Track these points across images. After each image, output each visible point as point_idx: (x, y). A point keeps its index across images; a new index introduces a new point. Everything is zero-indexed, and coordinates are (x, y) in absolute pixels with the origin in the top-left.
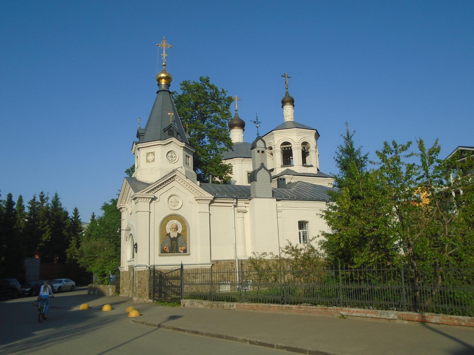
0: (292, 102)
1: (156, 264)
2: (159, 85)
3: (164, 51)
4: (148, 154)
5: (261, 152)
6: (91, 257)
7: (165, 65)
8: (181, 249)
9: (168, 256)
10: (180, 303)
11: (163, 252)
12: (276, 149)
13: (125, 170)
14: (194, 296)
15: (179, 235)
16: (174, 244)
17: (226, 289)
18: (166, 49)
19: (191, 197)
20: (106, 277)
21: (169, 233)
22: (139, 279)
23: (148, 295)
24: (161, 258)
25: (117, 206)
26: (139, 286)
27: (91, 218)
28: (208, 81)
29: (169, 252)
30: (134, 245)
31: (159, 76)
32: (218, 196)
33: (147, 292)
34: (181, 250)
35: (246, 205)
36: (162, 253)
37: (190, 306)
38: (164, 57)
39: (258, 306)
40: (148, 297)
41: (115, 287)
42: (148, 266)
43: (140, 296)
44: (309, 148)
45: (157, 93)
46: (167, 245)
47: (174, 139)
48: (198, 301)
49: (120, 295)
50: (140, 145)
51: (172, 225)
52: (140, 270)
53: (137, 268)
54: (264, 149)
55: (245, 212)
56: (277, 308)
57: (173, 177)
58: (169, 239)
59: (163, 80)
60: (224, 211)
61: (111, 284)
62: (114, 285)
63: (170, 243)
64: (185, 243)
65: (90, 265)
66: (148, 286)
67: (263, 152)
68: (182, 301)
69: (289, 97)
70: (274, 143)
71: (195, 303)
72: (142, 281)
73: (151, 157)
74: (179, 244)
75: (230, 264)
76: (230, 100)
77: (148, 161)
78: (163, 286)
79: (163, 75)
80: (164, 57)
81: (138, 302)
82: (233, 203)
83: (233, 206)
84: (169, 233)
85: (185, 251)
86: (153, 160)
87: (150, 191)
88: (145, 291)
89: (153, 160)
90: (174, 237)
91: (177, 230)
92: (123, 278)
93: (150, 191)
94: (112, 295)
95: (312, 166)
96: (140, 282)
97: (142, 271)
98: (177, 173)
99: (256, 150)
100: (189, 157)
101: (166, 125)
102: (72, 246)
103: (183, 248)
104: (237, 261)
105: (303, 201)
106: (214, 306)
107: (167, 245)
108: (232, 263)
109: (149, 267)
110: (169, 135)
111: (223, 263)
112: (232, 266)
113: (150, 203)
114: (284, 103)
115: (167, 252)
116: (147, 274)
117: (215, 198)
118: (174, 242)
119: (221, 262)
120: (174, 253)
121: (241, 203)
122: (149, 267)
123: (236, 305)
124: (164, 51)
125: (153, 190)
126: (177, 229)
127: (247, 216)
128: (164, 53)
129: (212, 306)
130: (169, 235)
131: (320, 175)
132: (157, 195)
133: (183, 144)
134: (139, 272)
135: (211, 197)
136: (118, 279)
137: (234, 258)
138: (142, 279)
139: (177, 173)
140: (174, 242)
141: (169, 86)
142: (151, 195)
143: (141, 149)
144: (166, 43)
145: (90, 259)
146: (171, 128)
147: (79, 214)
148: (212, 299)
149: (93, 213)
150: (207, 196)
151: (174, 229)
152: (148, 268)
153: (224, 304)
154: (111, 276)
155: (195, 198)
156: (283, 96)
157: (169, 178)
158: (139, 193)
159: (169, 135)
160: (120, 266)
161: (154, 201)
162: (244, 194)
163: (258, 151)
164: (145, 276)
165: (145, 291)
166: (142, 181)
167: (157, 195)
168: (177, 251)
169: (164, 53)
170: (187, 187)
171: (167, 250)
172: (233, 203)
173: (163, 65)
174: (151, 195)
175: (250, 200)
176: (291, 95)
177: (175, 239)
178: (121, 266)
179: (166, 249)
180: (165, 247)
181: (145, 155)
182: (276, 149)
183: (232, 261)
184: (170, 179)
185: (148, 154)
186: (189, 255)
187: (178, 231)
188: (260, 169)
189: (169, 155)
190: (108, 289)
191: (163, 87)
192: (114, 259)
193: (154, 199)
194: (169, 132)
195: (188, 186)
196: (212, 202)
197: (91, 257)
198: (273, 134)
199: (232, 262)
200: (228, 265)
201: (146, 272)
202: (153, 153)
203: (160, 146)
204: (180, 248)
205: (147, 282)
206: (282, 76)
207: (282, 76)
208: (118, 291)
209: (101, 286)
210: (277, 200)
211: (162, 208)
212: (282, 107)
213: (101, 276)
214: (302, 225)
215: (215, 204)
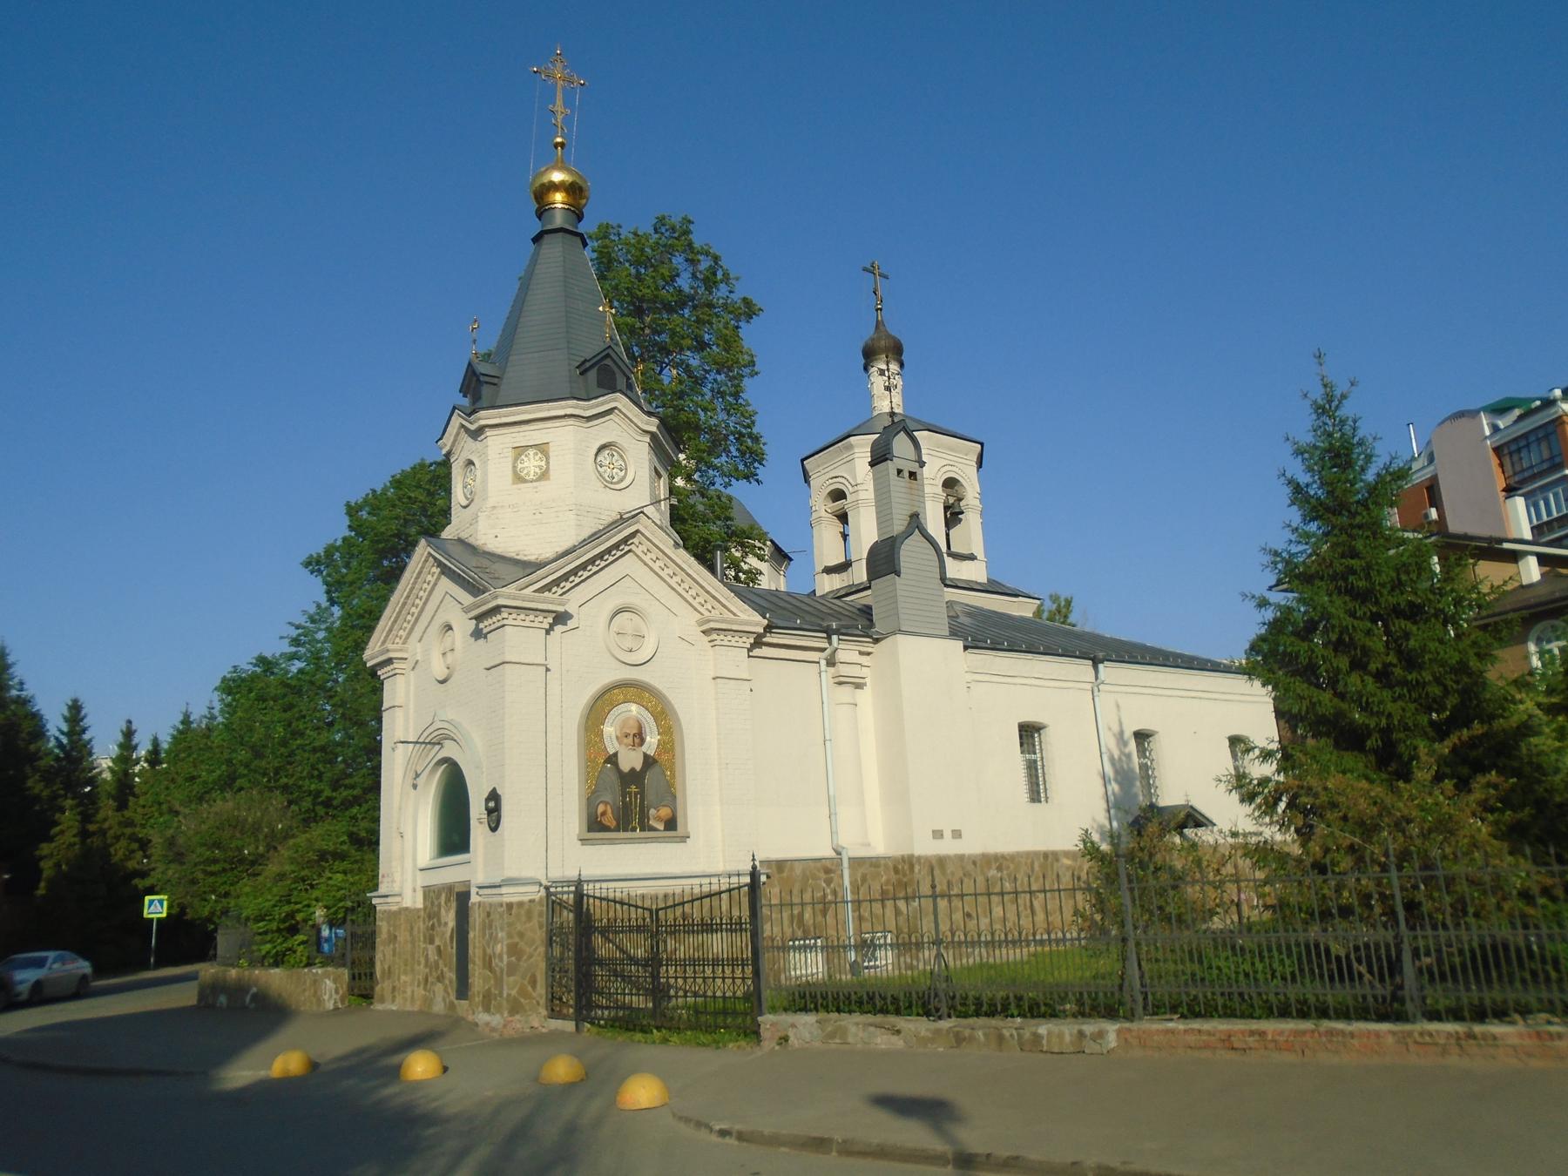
0: (896, 351)
1: (586, 874)
2: (543, 210)
3: (559, 95)
4: (520, 450)
5: (906, 474)
6: (215, 861)
7: (562, 145)
8: (656, 815)
9: (612, 841)
10: (754, 1033)
11: (594, 825)
12: (862, 495)
13: (304, 558)
14: (808, 999)
15: (649, 761)
16: (632, 797)
17: (809, 966)
18: (564, 88)
19: (687, 622)
20: (301, 938)
21: (615, 755)
22: (510, 936)
23: (543, 1001)
24: (589, 849)
25: (365, 657)
26: (509, 964)
27: (120, 738)
28: (687, 232)
29: (617, 830)
30: (488, 800)
31: (545, 180)
32: (780, 623)
33: (541, 990)
34: (659, 819)
35: (864, 660)
36: (590, 830)
37: (817, 1044)
38: (560, 117)
39: (1262, 1034)
40: (544, 1012)
41: (345, 973)
42: (545, 882)
43: (516, 1008)
44: (960, 500)
45: (537, 239)
46: (608, 798)
47: (620, 401)
48: (870, 1018)
49: (378, 1007)
50: (486, 417)
51: (625, 723)
52: (514, 899)
53: (504, 890)
54: (914, 467)
55: (859, 686)
56: (1390, 1040)
57: (625, 541)
58: (614, 779)
59: (559, 198)
60: (795, 678)
61: (323, 965)
62: (344, 965)
63: (618, 789)
64: (670, 795)
65: (213, 892)
66: (543, 965)
67: (912, 475)
68: (767, 1020)
69: (889, 336)
70: (855, 478)
71: (853, 1029)
72: (522, 945)
73: (531, 464)
74: (651, 796)
75: (823, 875)
76: (749, 310)
77: (519, 478)
78: (608, 967)
79: (557, 177)
80: (560, 117)
81: (509, 1032)
82: (823, 650)
83: (823, 663)
84: (615, 755)
85: (671, 824)
86: (544, 475)
87: (548, 588)
88: (534, 987)
89: (544, 475)
90: (633, 770)
91: (642, 741)
92: (393, 938)
93: (548, 588)
94: (336, 1009)
95: (972, 557)
96: (513, 950)
97: (521, 904)
98: (642, 525)
99: (891, 467)
100: (659, 476)
101: (590, 349)
102: (62, 832)
103: (665, 812)
104: (846, 864)
105: (1030, 656)
106: (971, 1039)
107: (608, 798)
108: (827, 871)
109: (547, 888)
110: (600, 384)
111: (798, 870)
112: (829, 882)
113: (548, 632)
114: (869, 355)
115: (605, 829)
116: (540, 915)
117: (769, 629)
118: (633, 788)
119: (792, 869)
120: (634, 830)
121: (848, 651)
122: (547, 888)
123: (1119, 1032)
124: (559, 95)
125: (556, 583)
126: (639, 738)
127: (865, 697)
128: (559, 102)
129: (959, 1040)
130: (613, 759)
131: (992, 588)
132: (572, 603)
133: (652, 425)
134: (510, 906)
135: (757, 622)
136: (366, 940)
137: (828, 853)
138: (521, 935)
139: (642, 525)
140: (633, 788)
141: (580, 217)
142: (551, 601)
143: (489, 432)
144: (565, 67)
145: (213, 868)
146: (608, 362)
147: (86, 723)
148: (944, 1010)
149: (129, 722)
150: (743, 616)
151: (630, 739)
152: (543, 892)
153: (1042, 1030)
154: (325, 932)
155: (700, 623)
156: (868, 333)
157: (608, 545)
158: (511, 589)
159: (600, 384)
160: (376, 887)
161: (559, 628)
162: (852, 619)
163: (899, 472)
164: (535, 922)
165: (533, 983)
166: (498, 551)
167: (572, 603)
168: (645, 826)
169: (559, 102)
170: (673, 582)
171: (609, 820)
172: (823, 650)
173: (556, 146)
174: (551, 601)
175: (877, 641)
176: (894, 329)
177: (634, 777)
178: (383, 889)
179: (604, 814)
180: (601, 809)
181: (510, 454)
182: (862, 495)
183: (828, 864)
184: (616, 546)
185: (520, 450)
186: (684, 838)
187: (644, 748)
188: (908, 534)
189: (605, 457)
190: (316, 981)
191: (559, 220)
192: (338, 865)
193: (561, 618)
194: (599, 376)
195: (678, 579)
196: (758, 643)
197: (215, 861)
198: (850, 447)
199: (827, 869)
200: (815, 878)
201: (537, 909)
202: (542, 449)
203: (571, 421)
204: (652, 811)
205: (542, 949)
206: (865, 269)
207: (865, 269)
208: (362, 988)
209: (276, 971)
210: (966, 648)
211: (583, 658)
212: (866, 369)
213: (279, 930)
214: (1029, 733)
215: (765, 651)
